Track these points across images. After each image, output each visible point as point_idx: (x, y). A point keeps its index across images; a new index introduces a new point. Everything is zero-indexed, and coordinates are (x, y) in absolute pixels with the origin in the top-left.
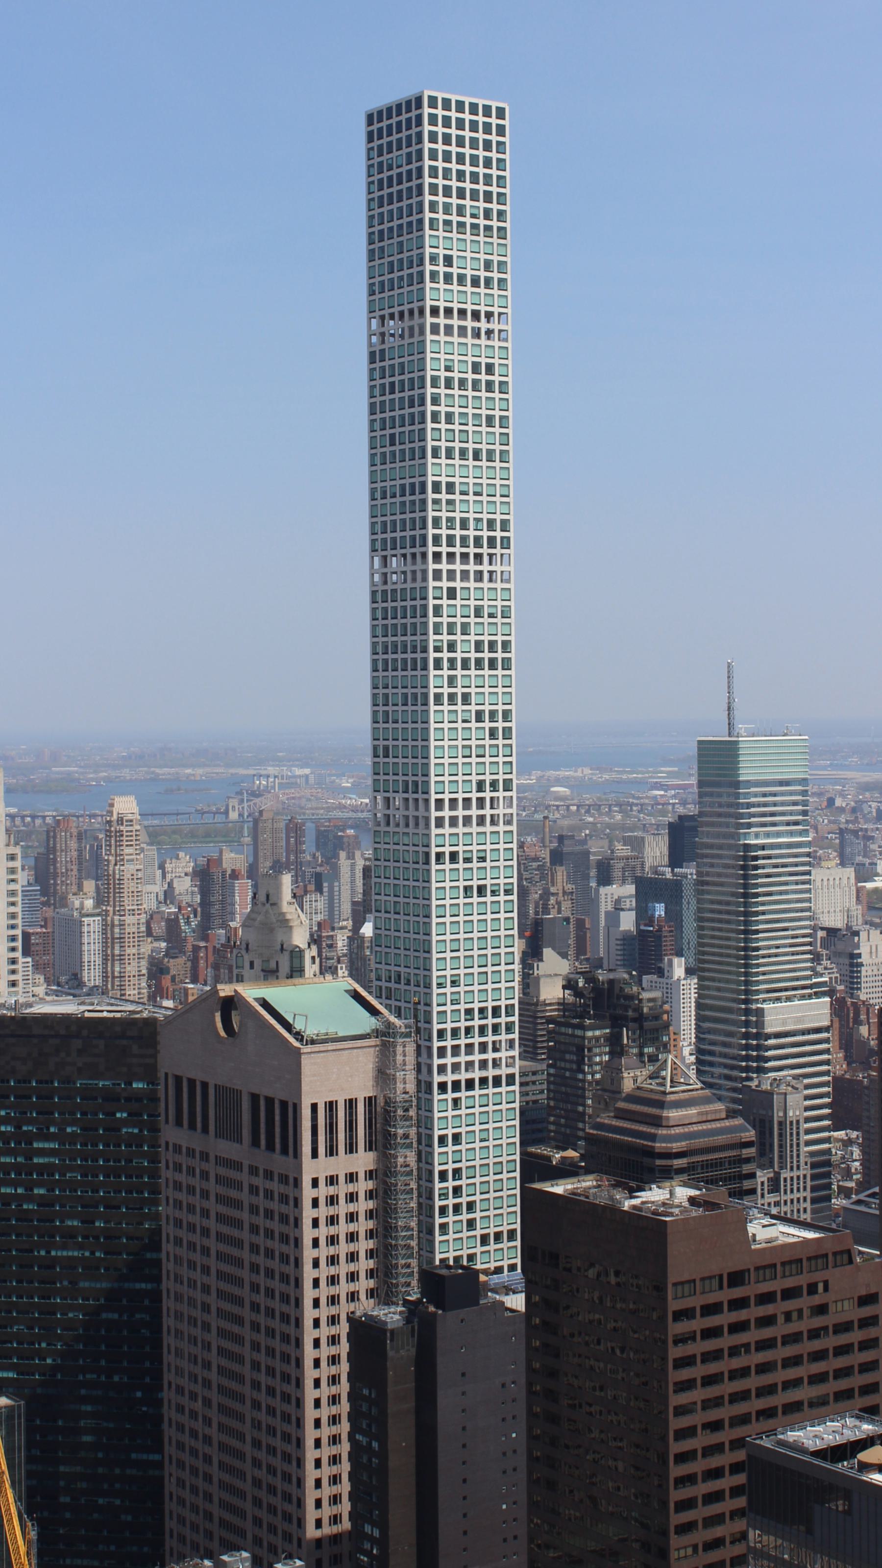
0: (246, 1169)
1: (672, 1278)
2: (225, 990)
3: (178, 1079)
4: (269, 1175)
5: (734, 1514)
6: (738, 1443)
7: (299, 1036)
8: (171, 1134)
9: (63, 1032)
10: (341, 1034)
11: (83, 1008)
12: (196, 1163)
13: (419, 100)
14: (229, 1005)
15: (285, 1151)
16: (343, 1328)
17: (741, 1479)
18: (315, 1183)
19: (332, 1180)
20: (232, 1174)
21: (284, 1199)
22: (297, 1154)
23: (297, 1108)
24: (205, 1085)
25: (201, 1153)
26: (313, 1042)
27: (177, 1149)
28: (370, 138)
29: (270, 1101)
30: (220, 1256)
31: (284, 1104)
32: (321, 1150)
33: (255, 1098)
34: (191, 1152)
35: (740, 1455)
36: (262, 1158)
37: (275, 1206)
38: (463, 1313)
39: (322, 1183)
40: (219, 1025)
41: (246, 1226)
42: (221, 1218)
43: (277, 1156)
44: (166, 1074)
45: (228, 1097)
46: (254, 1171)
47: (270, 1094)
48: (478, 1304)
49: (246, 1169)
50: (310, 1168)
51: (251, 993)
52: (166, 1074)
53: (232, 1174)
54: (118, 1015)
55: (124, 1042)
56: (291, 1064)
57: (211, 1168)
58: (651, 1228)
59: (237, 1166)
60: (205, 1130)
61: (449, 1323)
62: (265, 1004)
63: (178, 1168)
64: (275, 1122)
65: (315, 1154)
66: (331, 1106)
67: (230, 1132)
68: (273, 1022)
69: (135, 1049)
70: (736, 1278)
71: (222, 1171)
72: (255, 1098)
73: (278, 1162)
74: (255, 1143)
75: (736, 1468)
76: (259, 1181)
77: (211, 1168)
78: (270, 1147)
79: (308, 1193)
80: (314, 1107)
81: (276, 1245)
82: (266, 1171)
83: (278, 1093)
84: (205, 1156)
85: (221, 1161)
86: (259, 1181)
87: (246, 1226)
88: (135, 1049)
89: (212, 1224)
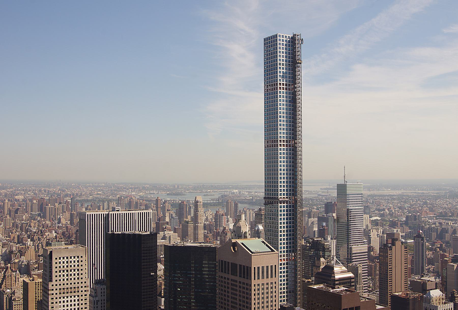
0: (238, 282)
2: (233, 241)
14: (235, 245)
15: (247, 278)
20: (235, 283)
21: (247, 289)
22: (251, 279)
23: (250, 268)
33: (240, 266)
34: (225, 278)
36: (242, 280)
37: (245, 291)
40: (232, 249)
41: (238, 295)
43: (246, 279)
45: (234, 266)
46: (240, 282)
47: (244, 265)
49: (238, 282)
51: (240, 241)
57: (230, 281)
58: (338, 297)
59: (236, 281)
62: (242, 244)
64: (246, 271)
65: (255, 279)
67: (234, 273)
68: (245, 248)
71: (233, 282)
73: (246, 281)
74: (240, 276)
79: (253, 288)
80: (255, 268)
84: (228, 279)
87: (238, 295)
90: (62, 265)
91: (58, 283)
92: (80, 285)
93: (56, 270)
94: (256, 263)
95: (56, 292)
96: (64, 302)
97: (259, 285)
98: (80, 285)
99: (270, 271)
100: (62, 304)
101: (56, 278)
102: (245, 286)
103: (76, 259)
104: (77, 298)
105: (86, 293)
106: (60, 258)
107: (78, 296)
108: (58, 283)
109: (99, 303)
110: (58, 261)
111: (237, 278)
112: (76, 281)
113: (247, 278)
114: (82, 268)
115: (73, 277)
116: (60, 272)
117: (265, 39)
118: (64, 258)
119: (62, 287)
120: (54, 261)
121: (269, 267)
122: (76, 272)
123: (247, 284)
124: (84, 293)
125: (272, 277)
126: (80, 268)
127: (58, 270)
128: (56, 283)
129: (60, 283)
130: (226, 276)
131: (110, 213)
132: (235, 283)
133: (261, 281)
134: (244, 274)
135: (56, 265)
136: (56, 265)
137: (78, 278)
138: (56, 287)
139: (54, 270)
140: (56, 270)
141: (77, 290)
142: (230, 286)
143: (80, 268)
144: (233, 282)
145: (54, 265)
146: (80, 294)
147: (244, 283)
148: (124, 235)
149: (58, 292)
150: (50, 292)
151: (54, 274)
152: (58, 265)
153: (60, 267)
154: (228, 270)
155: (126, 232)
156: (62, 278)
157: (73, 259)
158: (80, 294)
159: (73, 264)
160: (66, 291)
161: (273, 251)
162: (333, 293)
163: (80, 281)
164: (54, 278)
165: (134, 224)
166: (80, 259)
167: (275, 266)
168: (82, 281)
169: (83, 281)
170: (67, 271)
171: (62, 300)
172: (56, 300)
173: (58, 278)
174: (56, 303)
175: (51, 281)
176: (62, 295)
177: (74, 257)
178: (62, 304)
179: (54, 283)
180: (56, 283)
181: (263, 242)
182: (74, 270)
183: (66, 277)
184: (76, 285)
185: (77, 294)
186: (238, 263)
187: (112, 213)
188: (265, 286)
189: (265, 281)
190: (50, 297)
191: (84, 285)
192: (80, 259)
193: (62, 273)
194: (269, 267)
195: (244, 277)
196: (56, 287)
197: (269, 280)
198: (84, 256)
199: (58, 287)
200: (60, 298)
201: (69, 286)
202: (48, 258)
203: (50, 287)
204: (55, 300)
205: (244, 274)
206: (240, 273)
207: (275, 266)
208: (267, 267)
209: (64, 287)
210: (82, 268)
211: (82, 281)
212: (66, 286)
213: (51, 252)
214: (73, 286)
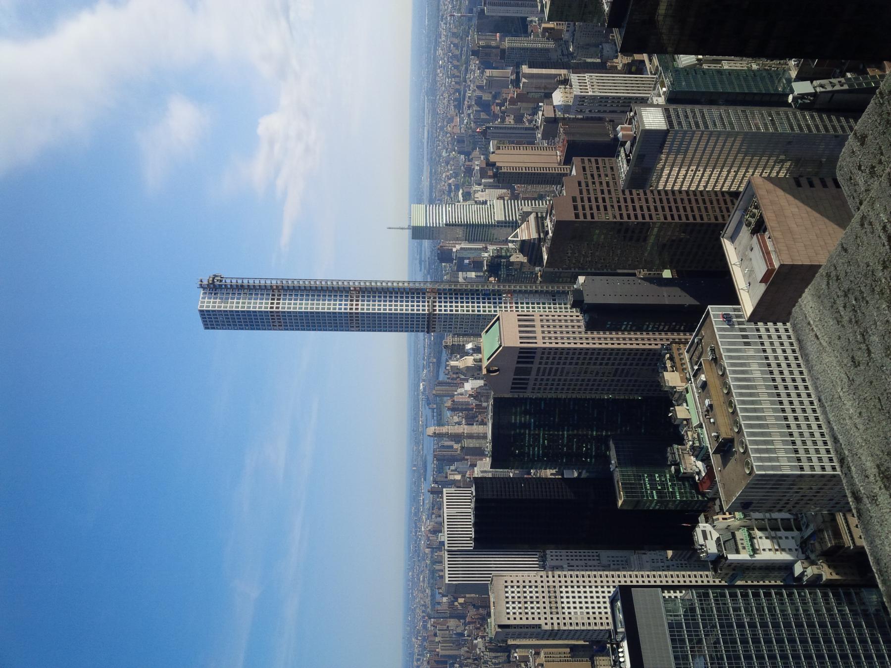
1: (573, 219)
2: (484, 372)
3: (512, 388)
5: (645, 194)
6: (623, 191)
7: (500, 346)
13: (201, 311)
14: (489, 371)
16: (589, 335)
17: (634, 191)
18: (544, 343)
20: (541, 371)
22: (536, 348)
23: (521, 348)
24: (514, 379)
28: (213, 328)
29: (519, 357)
31: (520, 352)
33: (518, 362)
35: (627, 192)
36: (537, 360)
38: (585, 295)
45: (518, 371)
50: (540, 344)
51: (485, 363)
53: (541, 371)
56: (507, 349)
57: (540, 377)
59: (539, 369)
60: (528, 379)
61: (588, 300)
64: (526, 355)
66: (521, 338)
67: (528, 372)
70: (574, 199)
72: (518, 362)
73: (538, 355)
74: (532, 363)
75: (631, 194)
78: (533, 357)
79: (547, 345)
81: (564, 356)
83: (517, 354)
90: (517, 611)
91: (542, 616)
92: (545, 584)
93: (524, 618)
94: (513, 340)
95: (555, 618)
96: (569, 608)
97: (544, 338)
98: (545, 584)
99: (525, 322)
100: (572, 610)
101: (537, 619)
103: (509, 589)
104: (564, 589)
105: (556, 576)
106: (508, 613)
107: (561, 587)
108: (542, 616)
109: (572, 563)
110: (511, 616)
111: (535, 367)
112: (540, 589)
113: (535, 353)
114: (521, 582)
115: (534, 595)
116: (527, 613)
117: (208, 328)
118: (508, 608)
119: (548, 610)
120: (512, 622)
122: (527, 589)
123: (543, 353)
124: (556, 579)
126: (521, 584)
127: (524, 617)
128: (542, 618)
129: (542, 613)
130: (531, 382)
131: (446, 548)
133: (539, 335)
135: (518, 619)
136: (518, 619)
137: (536, 587)
138: (549, 618)
139: (524, 622)
140: (524, 618)
141: (552, 589)
142: (545, 378)
143: (521, 584)
145: (518, 622)
146: (557, 584)
147: (542, 358)
148: (476, 525)
149: (555, 616)
150: (556, 627)
151: (531, 622)
152: (518, 616)
153: (520, 613)
155: (473, 520)
156: (535, 611)
157: (509, 595)
158: (557, 584)
159: (516, 595)
160: (553, 605)
161: (498, 319)
162: (554, 233)
163: (539, 584)
164: (536, 622)
165: (459, 511)
166: (509, 584)
168: (539, 582)
169: (539, 580)
170: (526, 603)
171: (566, 610)
172: (567, 618)
173: (536, 616)
174: (570, 618)
175: (539, 626)
176: (560, 610)
177: (507, 592)
178: (572, 610)
179: (542, 622)
180: (542, 618)
181: (487, 332)
182: (525, 592)
183: (535, 605)
184: (546, 589)
185: (557, 589)
186: (515, 365)
187: (446, 545)
188: (546, 329)
189: (538, 329)
190: (563, 628)
191: (545, 579)
192: (509, 584)
193: (529, 611)
195: (533, 357)
196: (549, 618)
197: (538, 323)
198: (505, 578)
199: (549, 616)
200: (564, 613)
201: (547, 600)
202: (507, 630)
203: (548, 627)
204: (567, 621)
208: (520, 326)
209: (548, 608)
210: (521, 582)
211: (539, 582)
212: (547, 605)
213: (500, 626)
214: (546, 594)
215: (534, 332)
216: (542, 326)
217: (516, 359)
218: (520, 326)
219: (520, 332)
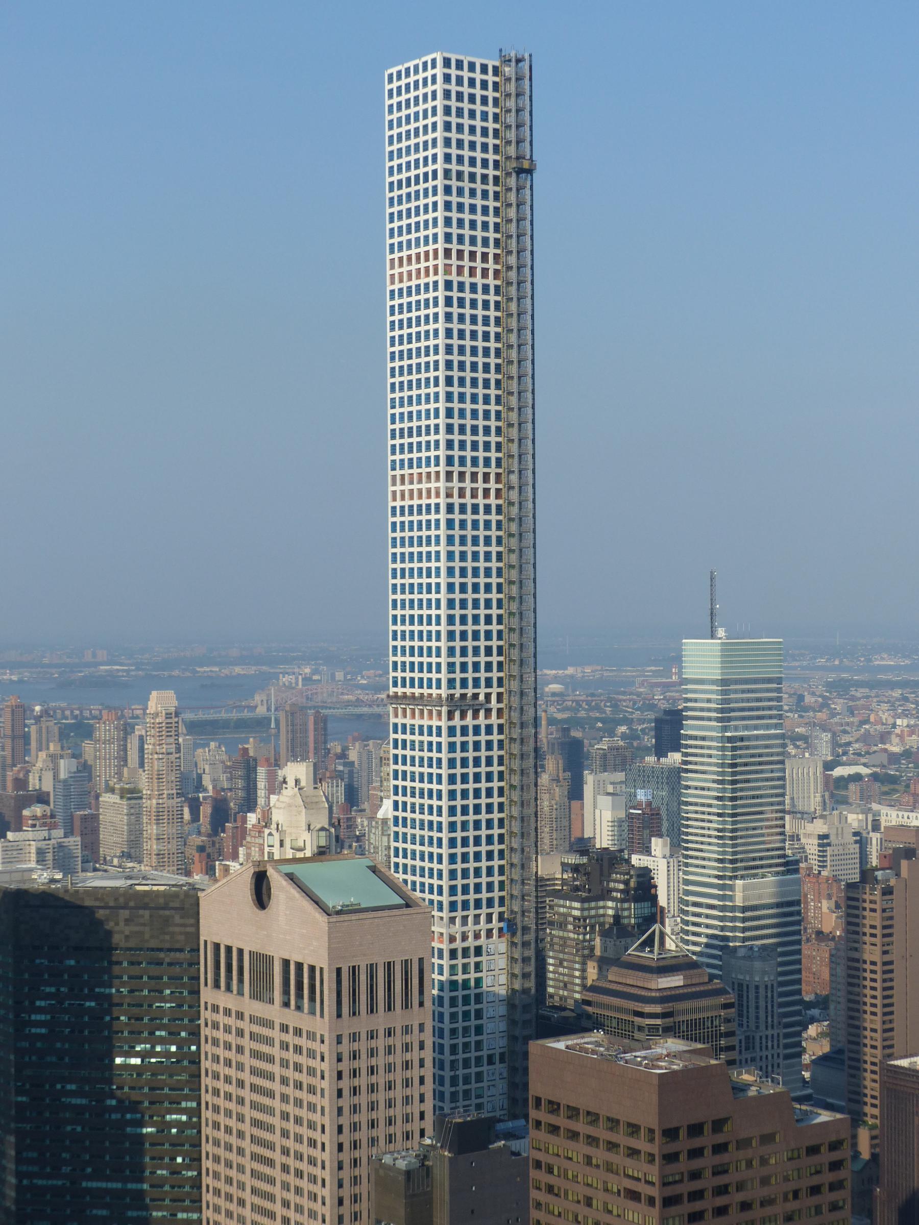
3: (217, 946)
4: (298, 1032)
8: (207, 995)
9: (112, 904)
10: (363, 906)
11: (130, 882)
12: (231, 1021)
16: (363, 1171)
19: (354, 1037)
20: (265, 1031)
24: (241, 952)
25: (237, 1013)
26: (339, 913)
27: (215, 1009)
29: (299, 966)
30: (254, 1106)
32: (345, 1010)
33: (286, 963)
34: (228, 1012)
36: (291, 1017)
39: (345, 1040)
41: (278, 1079)
42: (254, 1071)
44: (206, 942)
45: (262, 961)
46: (284, 1028)
48: (486, 1148)
49: (277, 1027)
52: (206, 942)
54: (162, 888)
55: (167, 913)
57: (245, 1025)
59: (269, 1024)
60: (240, 993)
63: (216, 1026)
67: (261, 992)
69: (177, 919)
71: (256, 1029)
72: (286, 963)
73: (304, 1021)
74: (286, 1004)
76: (289, 1038)
77: (245, 1025)
82: (295, 1029)
84: (240, 1016)
85: (253, 1020)
86: (289, 1038)
88: (177, 919)
89: (246, 1076)
102: (303, 1042)
111: (274, 1012)
121: (398, 968)
125: (407, 1005)
132: (265, 1031)
134: (300, 995)
144: (256, 1029)
147: (298, 1032)
154: (241, 981)
167: (421, 960)
181: (374, 869)
186: (278, 953)
188: (380, 1043)
189: (381, 1021)
194: (398, 968)
205: (300, 995)
206: (286, 991)
207: (421, 960)
208: (389, 966)
215: (372, 1010)
216: (389, 1033)
217: (295, 957)
218: (389, 966)
219: (372, 969)
